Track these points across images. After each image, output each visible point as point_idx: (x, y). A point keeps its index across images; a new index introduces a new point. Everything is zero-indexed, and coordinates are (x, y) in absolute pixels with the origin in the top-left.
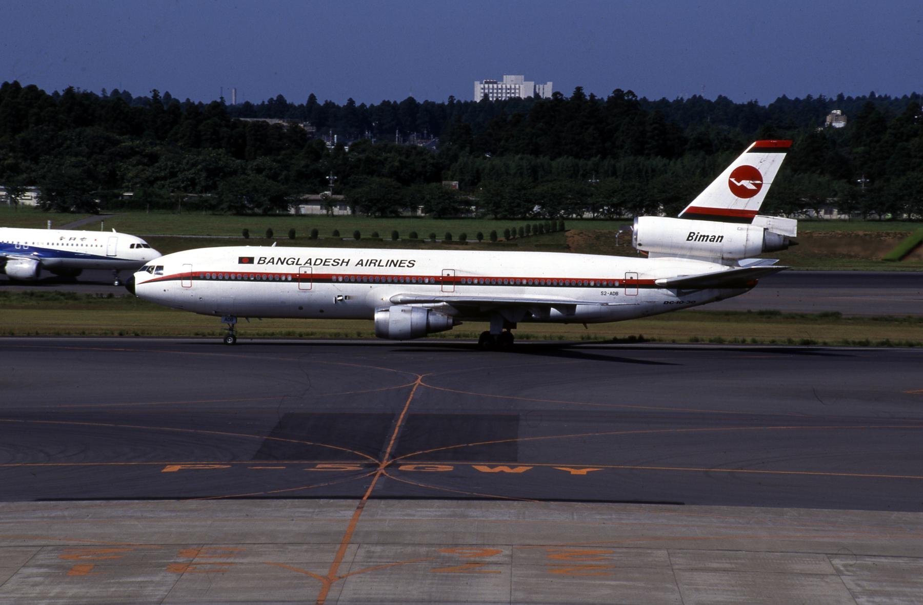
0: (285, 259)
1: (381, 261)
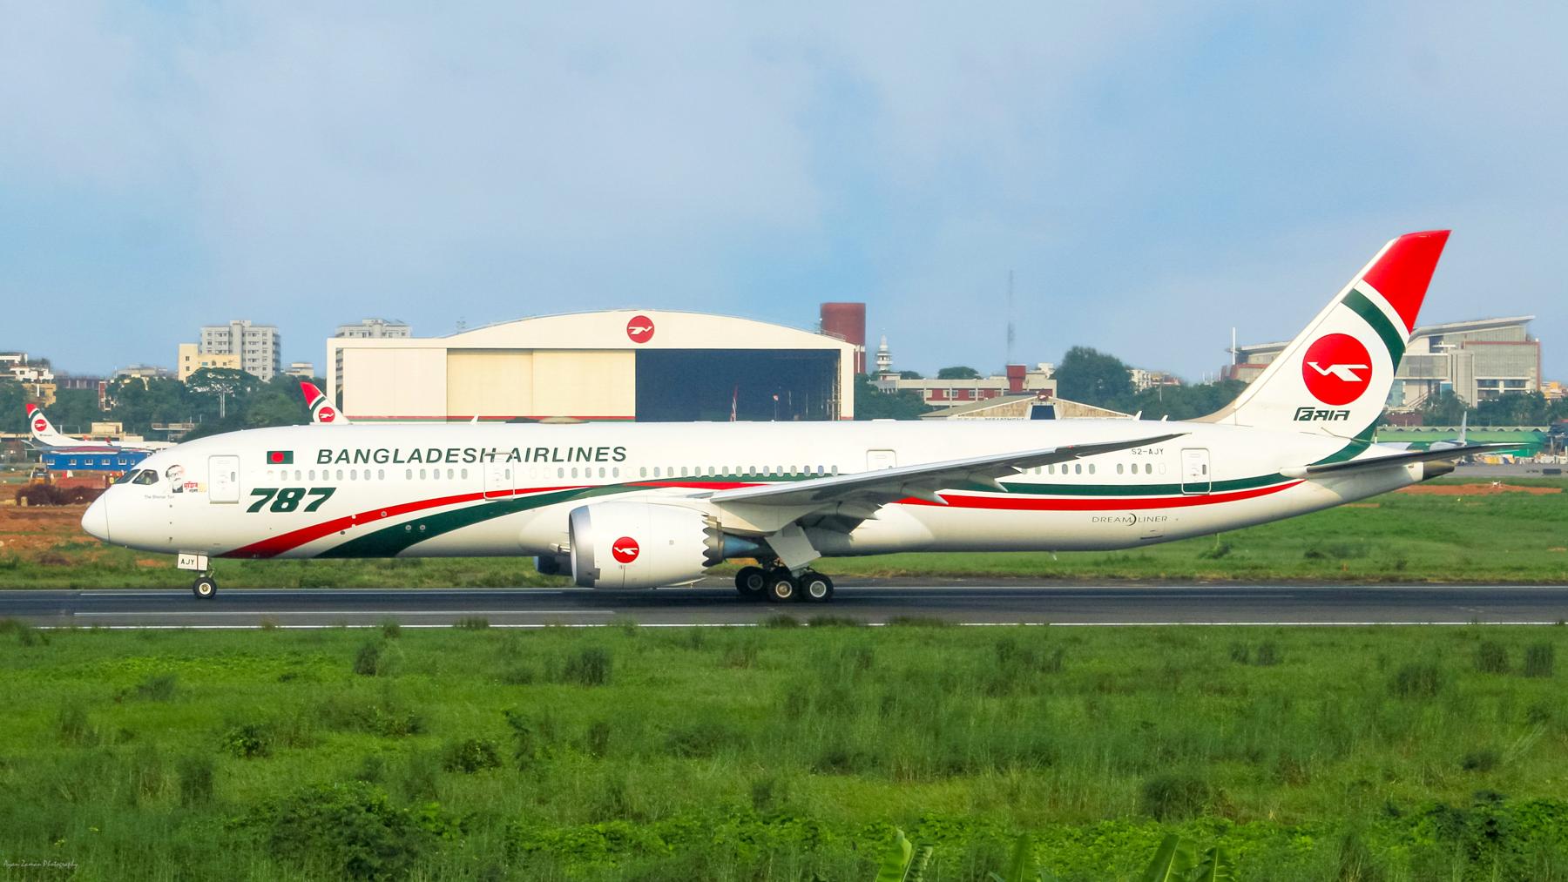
0: (369, 451)
1: (556, 449)
